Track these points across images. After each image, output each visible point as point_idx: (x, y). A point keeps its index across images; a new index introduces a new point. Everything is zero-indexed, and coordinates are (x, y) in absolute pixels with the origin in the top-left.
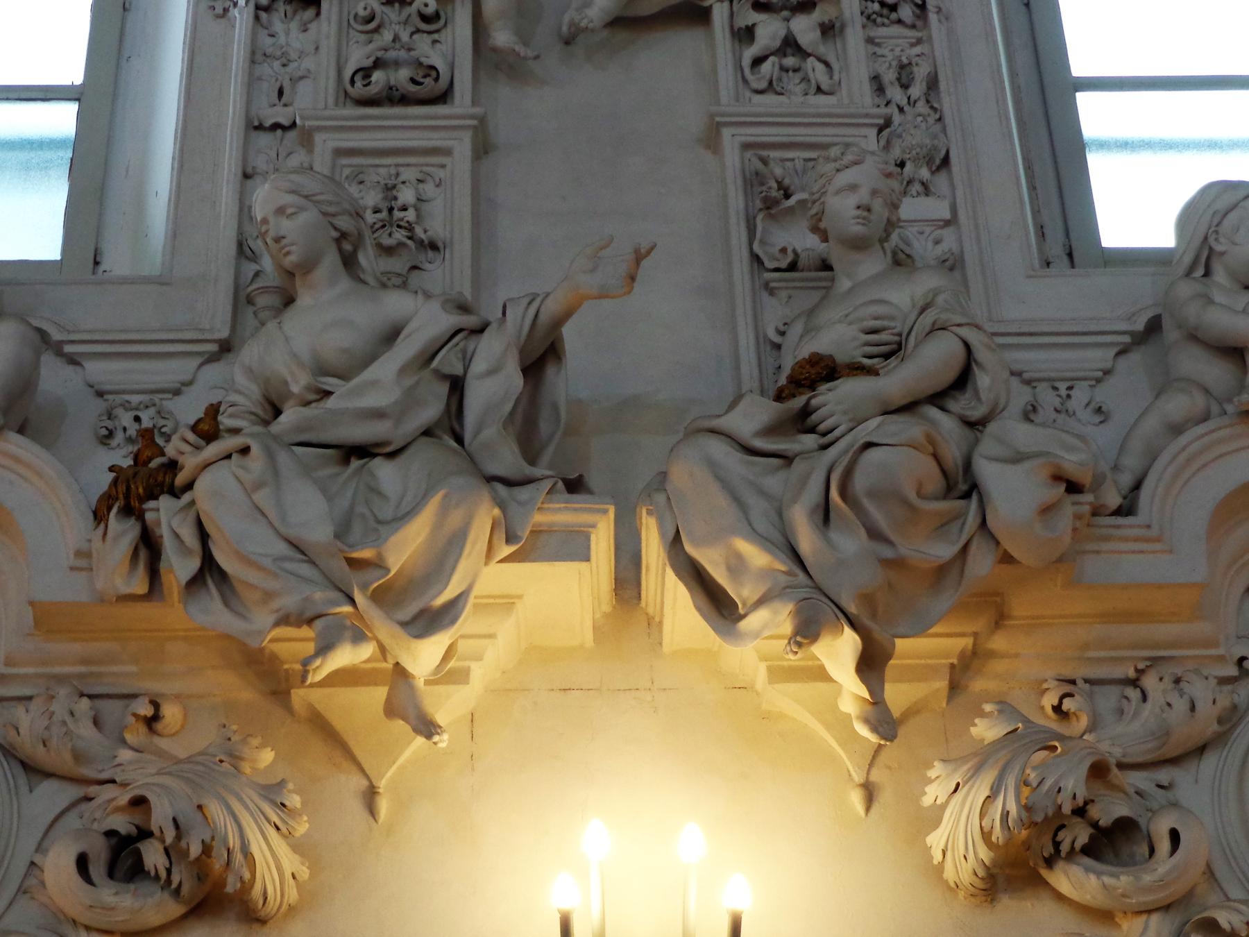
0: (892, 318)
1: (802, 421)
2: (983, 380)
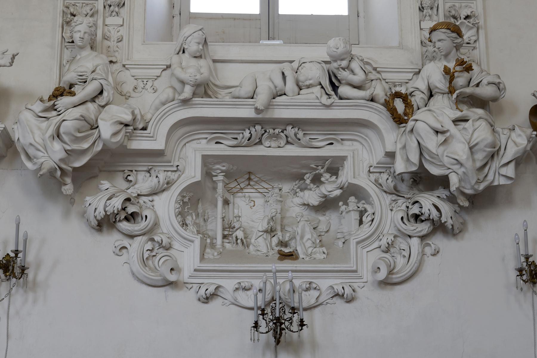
0: (86, 72)
1: (53, 108)
2: (105, 94)
